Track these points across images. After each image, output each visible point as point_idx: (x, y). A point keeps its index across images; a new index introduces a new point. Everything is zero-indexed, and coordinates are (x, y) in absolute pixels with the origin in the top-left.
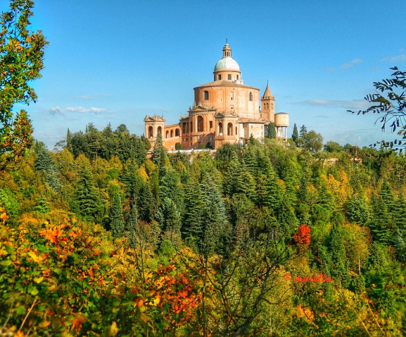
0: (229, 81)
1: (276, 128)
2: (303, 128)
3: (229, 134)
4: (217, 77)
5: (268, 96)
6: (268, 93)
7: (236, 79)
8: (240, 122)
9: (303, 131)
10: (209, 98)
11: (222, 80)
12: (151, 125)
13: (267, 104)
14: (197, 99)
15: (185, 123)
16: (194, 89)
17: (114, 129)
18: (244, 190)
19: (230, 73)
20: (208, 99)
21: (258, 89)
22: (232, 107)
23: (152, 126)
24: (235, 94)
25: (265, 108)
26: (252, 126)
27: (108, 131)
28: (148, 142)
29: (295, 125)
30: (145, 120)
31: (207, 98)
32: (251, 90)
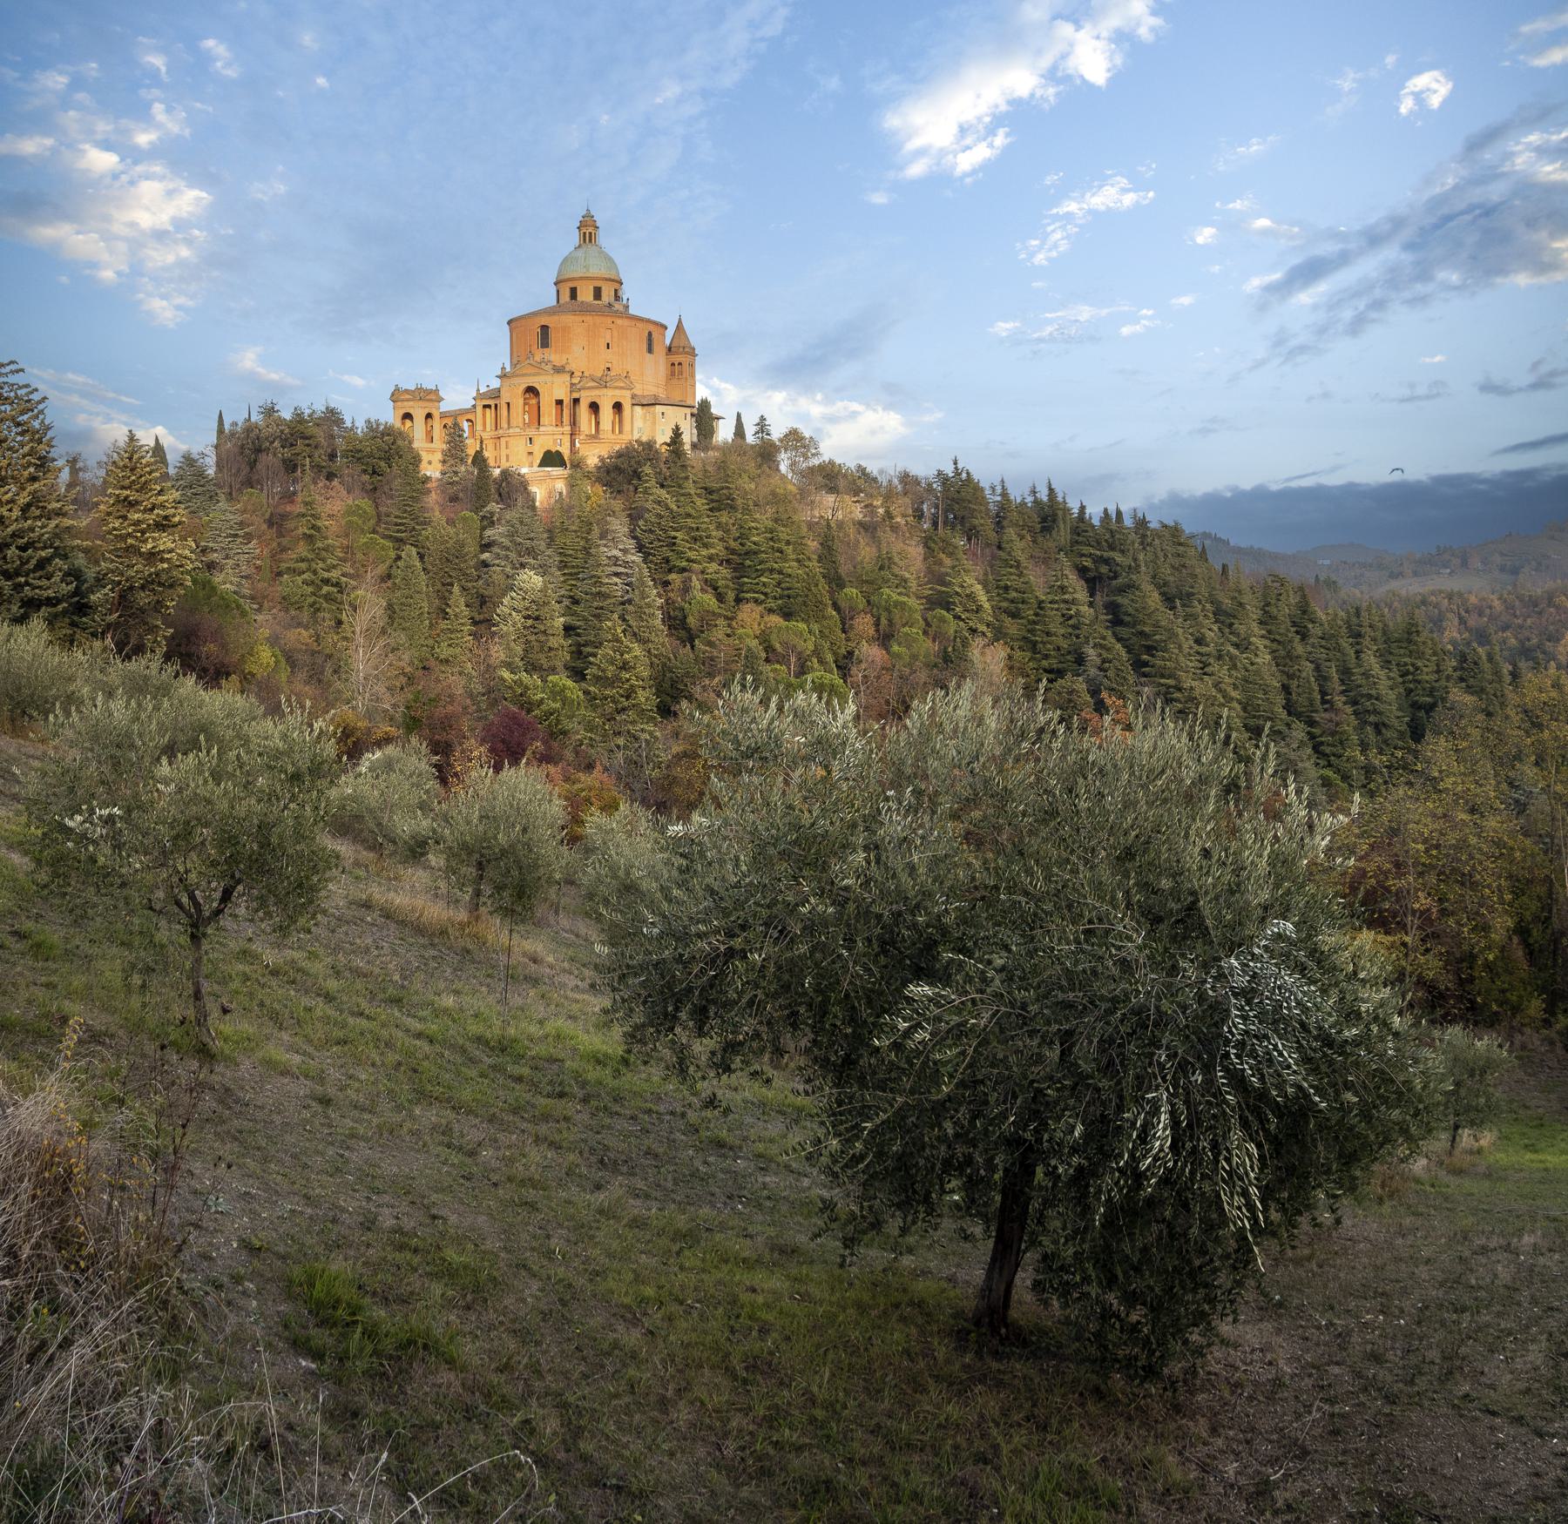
2: (762, 425)
13: (680, 364)
19: (598, 284)
22: (609, 365)
23: (411, 412)
24: (615, 334)
25: (673, 374)
29: (739, 416)
32: (651, 328)
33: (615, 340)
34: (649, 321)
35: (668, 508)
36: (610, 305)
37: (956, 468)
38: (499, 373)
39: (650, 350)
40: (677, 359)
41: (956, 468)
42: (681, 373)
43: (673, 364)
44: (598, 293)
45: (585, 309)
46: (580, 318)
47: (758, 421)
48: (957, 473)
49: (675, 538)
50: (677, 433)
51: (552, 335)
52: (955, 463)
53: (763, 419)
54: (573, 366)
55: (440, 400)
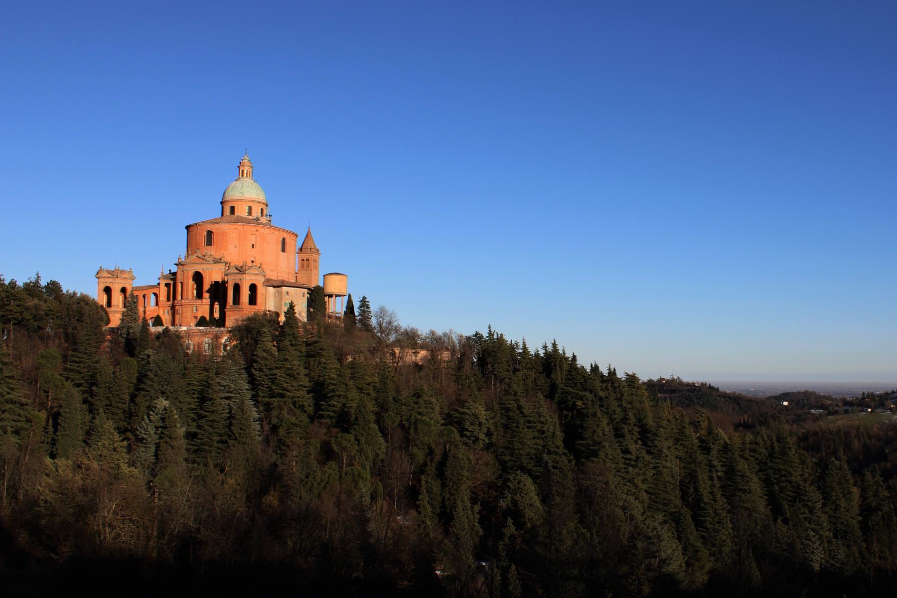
1: (326, 299)
2: (364, 303)
7: (260, 215)
8: (268, 284)
12: (108, 285)
13: (307, 260)
16: (188, 227)
19: (251, 204)
20: (211, 245)
21: (296, 233)
22: (253, 259)
23: (111, 285)
24: (259, 238)
25: (303, 266)
26: (287, 293)
30: (97, 276)
31: (209, 242)
32: (285, 235)
34: (284, 230)
35: (272, 355)
36: (257, 219)
37: (490, 331)
38: (176, 262)
39: (283, 250)
40: (305, 256)
41: (490, 331)
42: (308, 266)
43: (303, 260)
45: (241, 220)
46: (233, 227)
47: (361, 299)
48: (491, 334)
49: (276, 374)
50: (292, 307)
51: (214, 237)
52: (490, 328)
53: (364, 298)
54: (228, 259)
55: (133, 278)
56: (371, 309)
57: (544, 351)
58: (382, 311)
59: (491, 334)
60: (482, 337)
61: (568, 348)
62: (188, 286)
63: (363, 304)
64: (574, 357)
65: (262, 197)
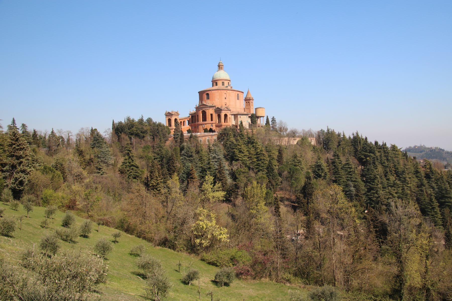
0: (223, 86)
2: (273, 119)
3: (225, 122)
4: (215, 84)
5: (249, 97)
6: (249, 95)
9: (273, 121)
10: (210, 98)
11: (218, 86)
14: (201, 99)
15: (193, 116)
16: (199, 92)
17: (145, 119)
18: (240, 159)
20: (209, 99)
22: (226, 104)
23: (170, 118)
25: (247, 105)
27: (141, 121)
28: (169, 129)
31: (208, 98)
33: (227, 96)
34: (237, 91)
38: (195, 107)
39: (238, 99)
44: (223, 84)
53: (273, 117)
56: (277, 122)
57: (353, 136)
58: (281, 122)
59: (328, 130)
60: (324, 131)
61: (363, 134)
62: (200, 116)
63: (273, 120)
64: (366, 138)
65: (228, 78)
